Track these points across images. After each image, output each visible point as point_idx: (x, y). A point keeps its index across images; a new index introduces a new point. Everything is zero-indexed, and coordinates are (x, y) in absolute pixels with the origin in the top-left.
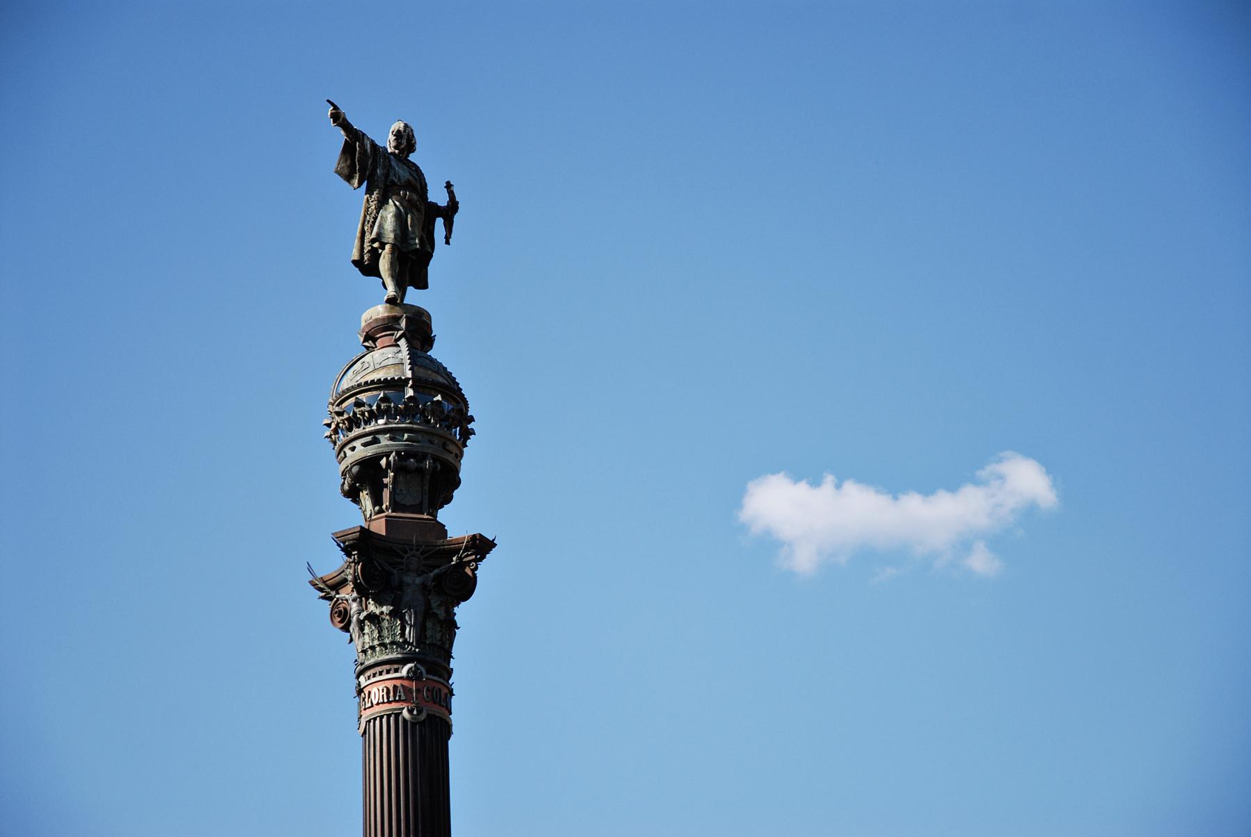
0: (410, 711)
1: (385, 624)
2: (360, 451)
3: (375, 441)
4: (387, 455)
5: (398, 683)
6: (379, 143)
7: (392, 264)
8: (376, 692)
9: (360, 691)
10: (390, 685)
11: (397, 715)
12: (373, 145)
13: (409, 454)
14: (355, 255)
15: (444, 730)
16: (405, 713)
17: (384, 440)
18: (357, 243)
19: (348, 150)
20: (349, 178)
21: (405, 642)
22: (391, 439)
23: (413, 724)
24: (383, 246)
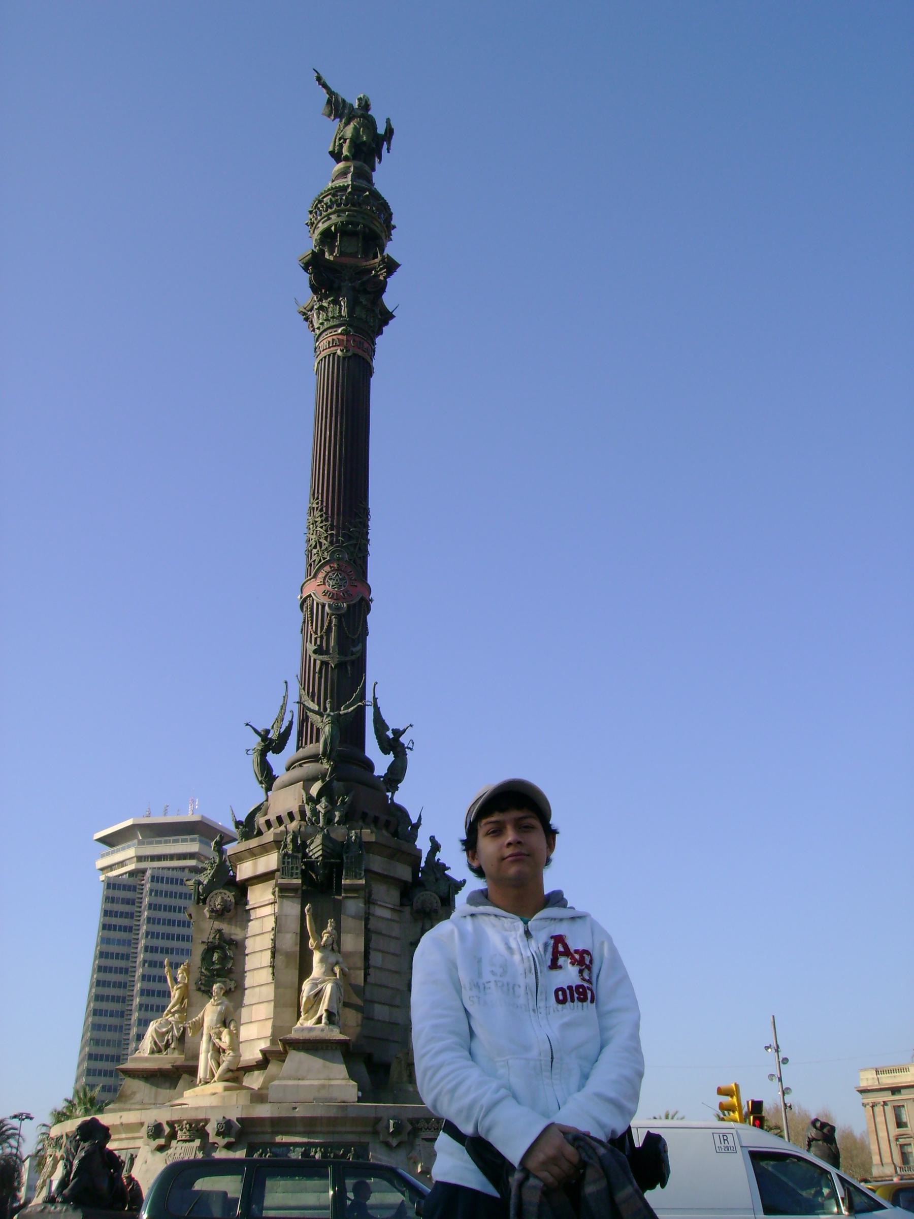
0: (342, 351)
1: (330, 309)
2: (322, 226)
3: (329, 219)
5: (335, 337)
6: (348, 101)
7: (349, 147)
8: (323, 344)
9: (316, 348)
10: (330, 339)
11: (334, 354)
12: (344, 101)
13: (348, 223)
14: (331, 149)
15: (368, 371)
16: (339, 353)
17: (333, 217)
18: (332, 144)
19: (329, 102)
20: (329, 116)
21: (341, 316)
22: (339, 216)
23: (344, 358)
24: (345, 142)
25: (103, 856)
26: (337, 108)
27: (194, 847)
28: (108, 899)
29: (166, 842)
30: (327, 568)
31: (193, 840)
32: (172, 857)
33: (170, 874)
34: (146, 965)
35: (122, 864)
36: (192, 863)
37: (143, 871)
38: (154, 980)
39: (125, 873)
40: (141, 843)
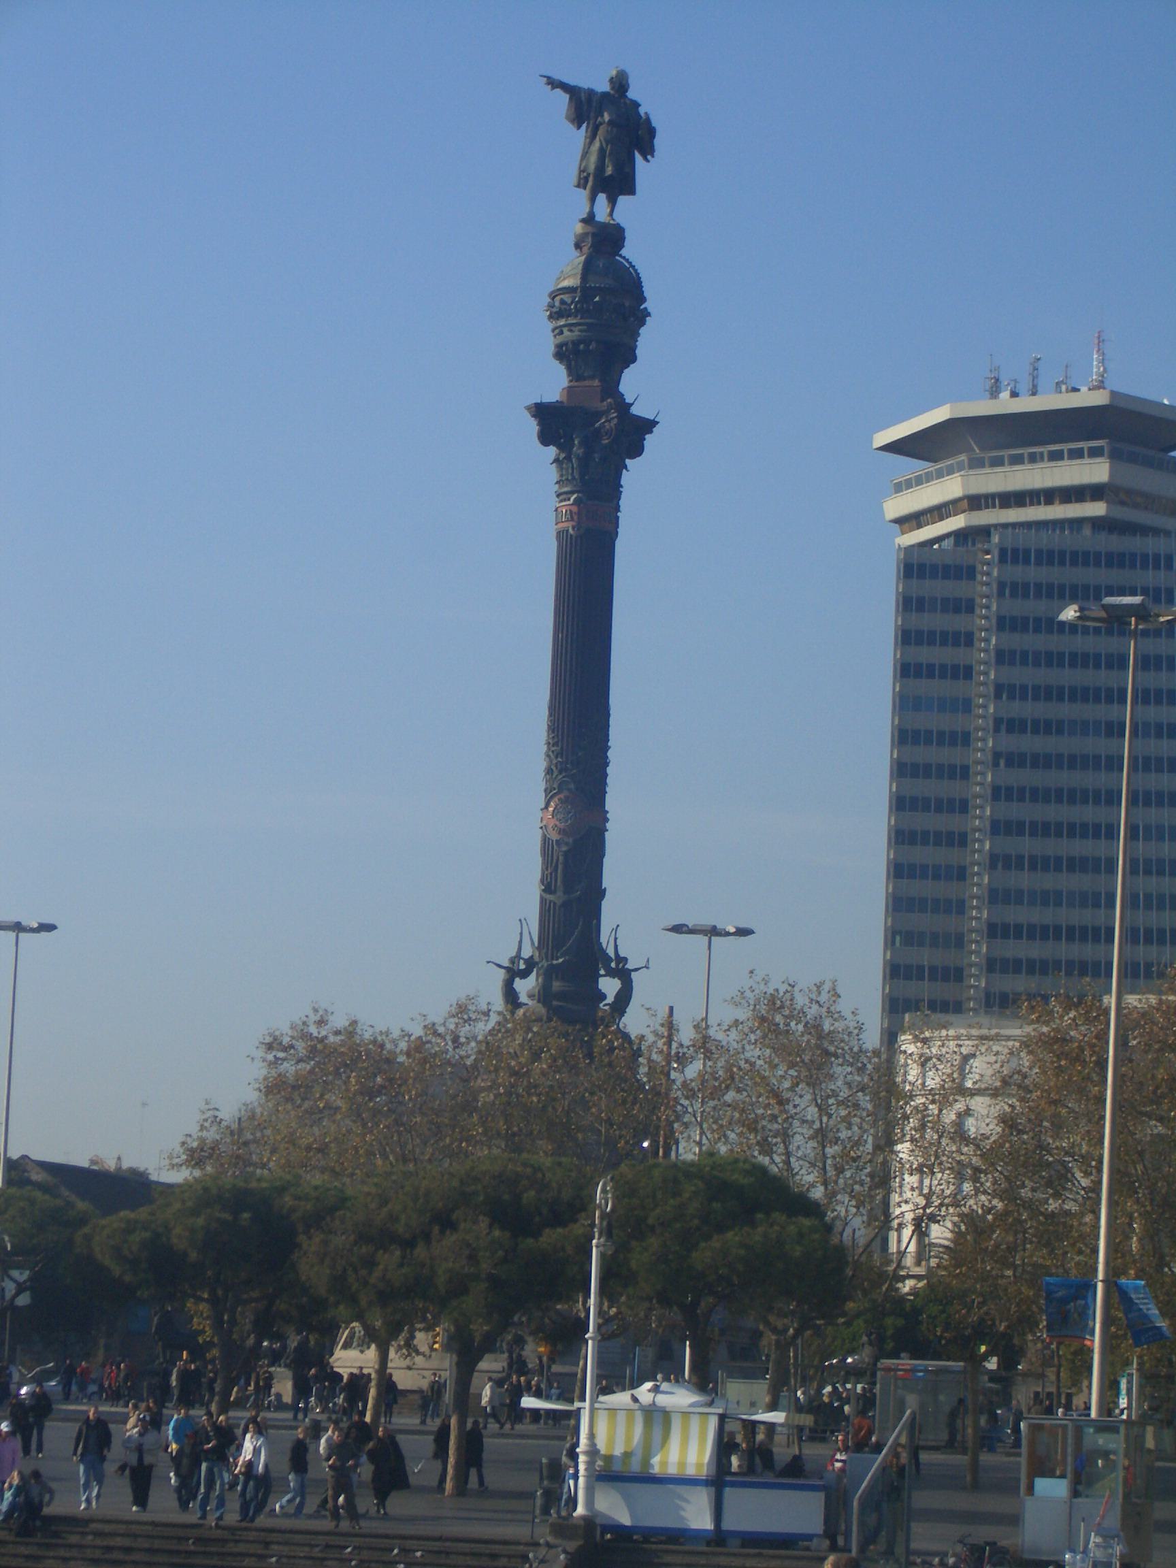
4: (566, 344)
25: (898, 488)
26: (584, 107)
27: (1097, 471)
28: (908, 604)
29: (1033, 459)
30: (556, 799)
31: (1095, 453)
32: (1049, 496)
33: (1045, 540)
34: (1002, 762)
35: (940, 512)
36: (1097, 509)
37: (984, 532)
38: (1021, 799)
39: (947, 535)
40: (976, 463)
